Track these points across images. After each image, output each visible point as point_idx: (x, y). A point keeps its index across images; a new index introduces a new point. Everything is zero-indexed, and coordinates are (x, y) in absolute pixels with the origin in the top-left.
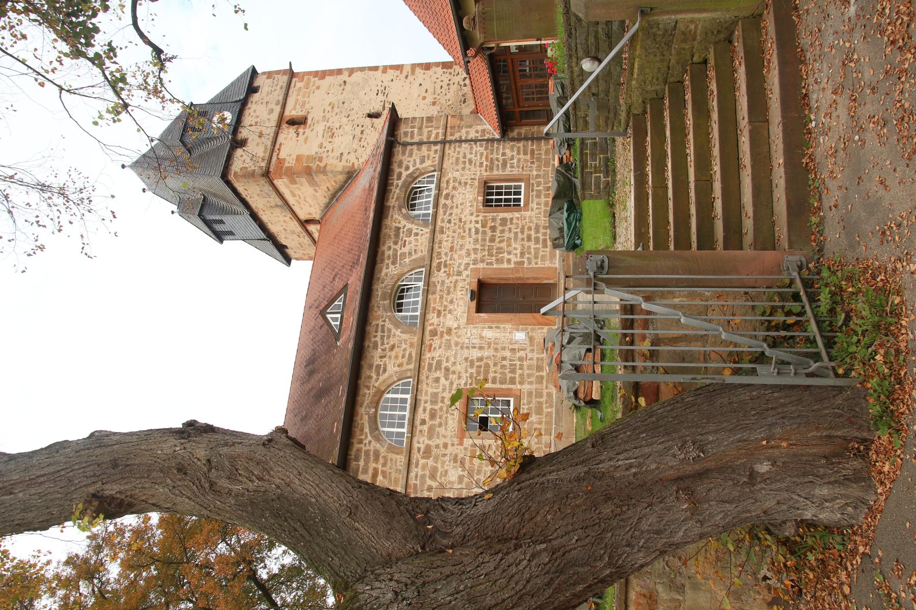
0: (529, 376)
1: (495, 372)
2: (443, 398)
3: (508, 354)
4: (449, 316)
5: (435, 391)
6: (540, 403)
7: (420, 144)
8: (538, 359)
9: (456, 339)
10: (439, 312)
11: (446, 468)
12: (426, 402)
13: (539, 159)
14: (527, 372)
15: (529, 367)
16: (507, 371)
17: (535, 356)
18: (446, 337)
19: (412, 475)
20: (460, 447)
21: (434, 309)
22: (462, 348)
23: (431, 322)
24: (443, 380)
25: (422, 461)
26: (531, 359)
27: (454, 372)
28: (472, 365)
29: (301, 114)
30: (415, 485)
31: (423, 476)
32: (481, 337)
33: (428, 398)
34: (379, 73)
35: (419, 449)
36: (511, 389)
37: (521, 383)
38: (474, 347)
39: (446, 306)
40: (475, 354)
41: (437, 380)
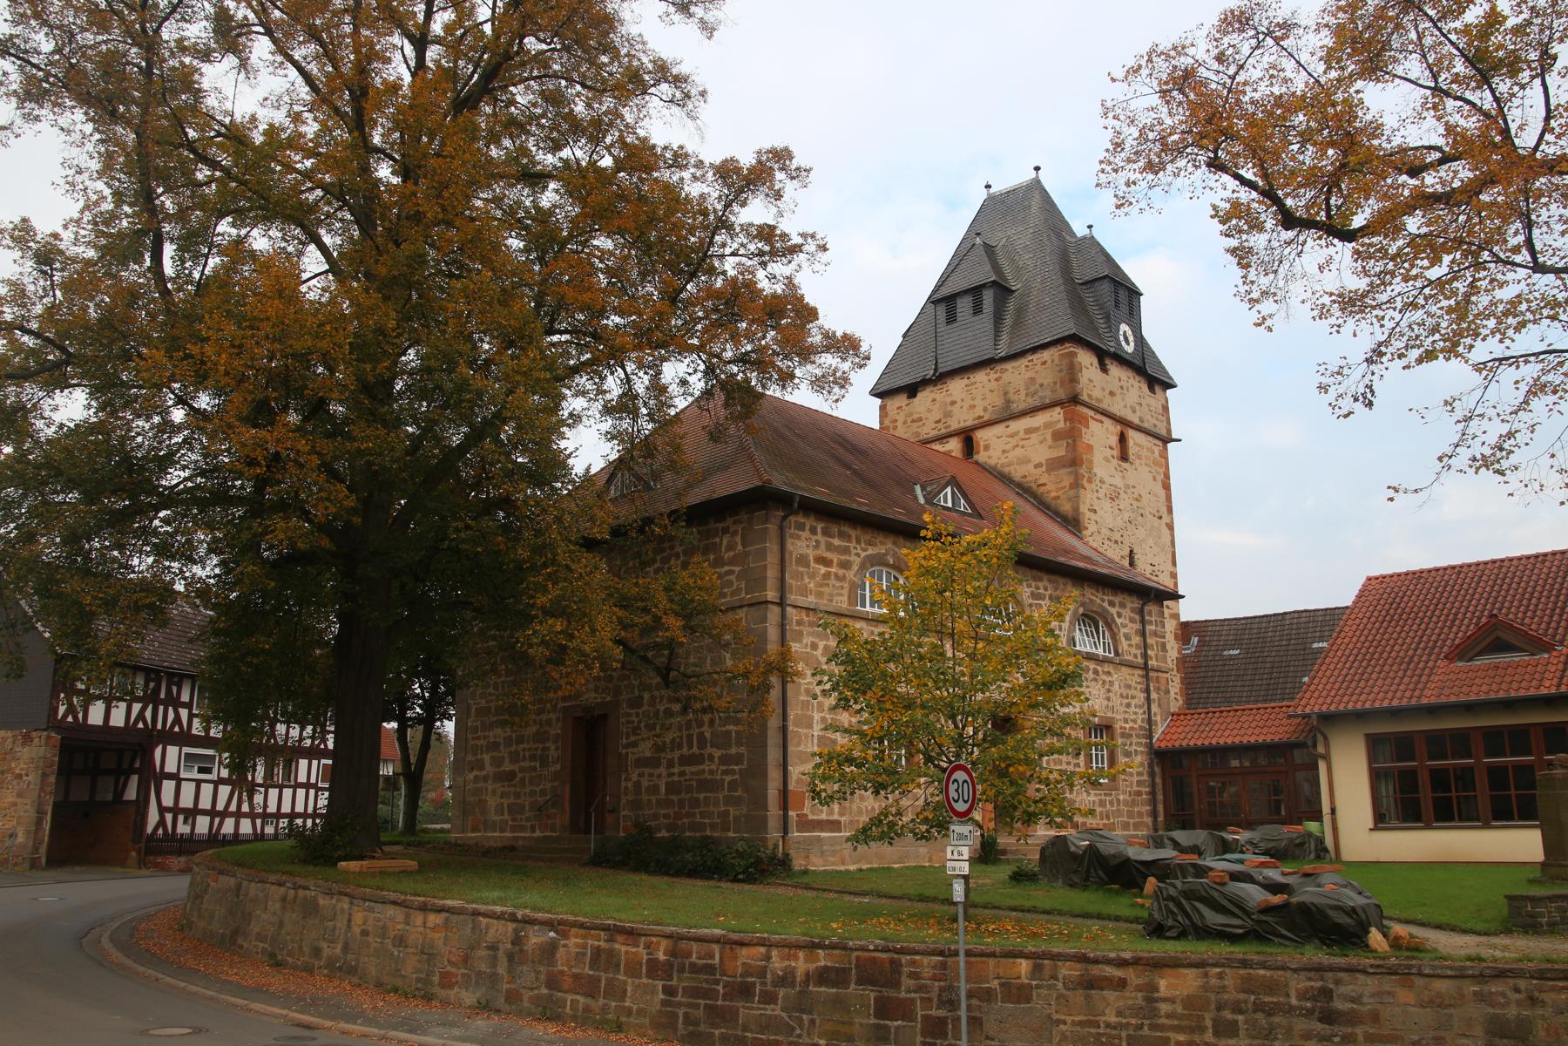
7: (1143, 634)
13: (1134, 803)
34: (1171, 568)
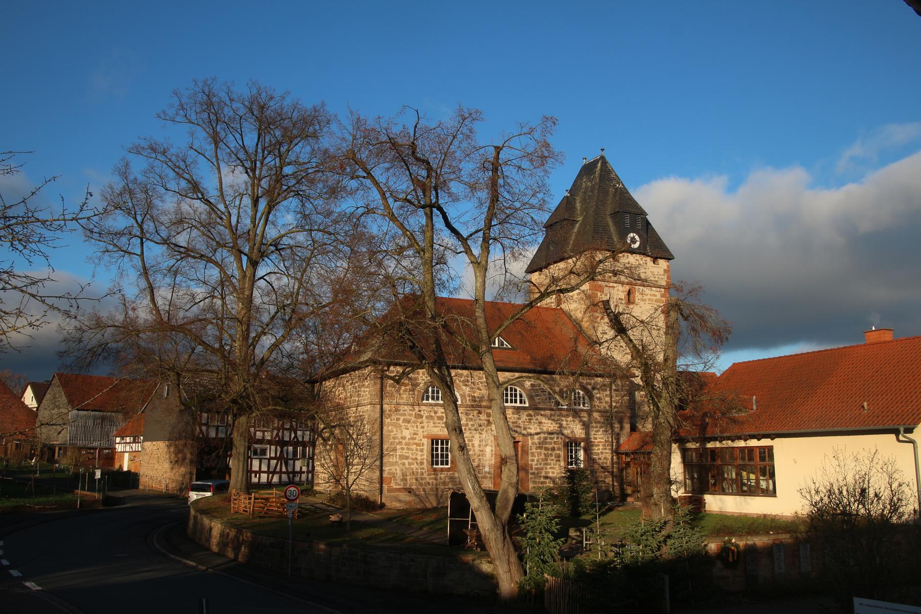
29: (637, 301)
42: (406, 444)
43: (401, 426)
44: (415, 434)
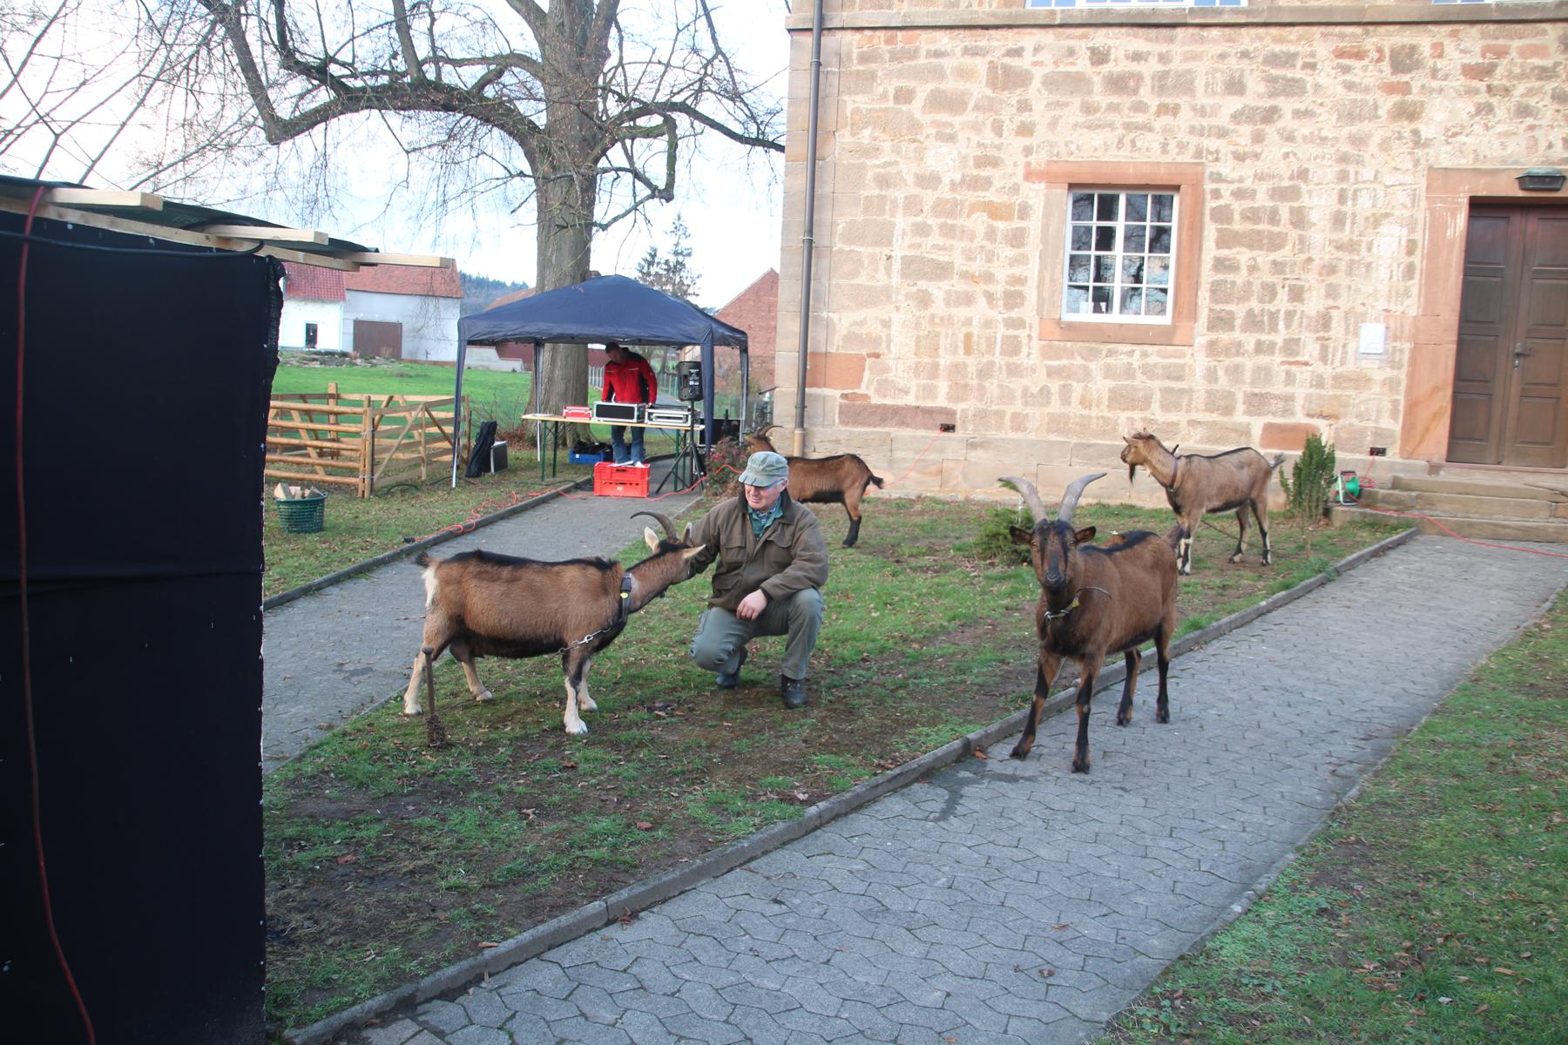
0: (1235, 372)
1: (1253, 268)
2: (1174, 111)
3: (1314, 304)
4: (1467, 106)
5: (1200, 84)
6: (1146, 402)
8: (1289, 399)
9: (1376, 139)
10: (1488, 71)
11: (961, 136)
12: (1163, 58)
14: (1248, 363)
15: (1263, 373)
16: (1254, 304)
17: (1300, 392)
18: (1387, 103)
19: (944, 40)
20: (1021, 171)
21: (1501, 53)
22: (1343, 159)
23: (1450, 47)
24: (1234, 104)
25: (981, 64)
26: (1290, 379)
27: (1258, 138)
28: (1280, 194)
30: (913, 54)
31: (938, 73)
32: (1376, 221)
33: (1176, 65)
35: (1017, 52)
36: (1194, 317)
37: (1212, 348)
38: (1342, 198)
39: (1507, 91)
40: (1319, 203)
41: (1235, 86)
42: (940, 208)
43: (915, 126)
44: (985, 161)
